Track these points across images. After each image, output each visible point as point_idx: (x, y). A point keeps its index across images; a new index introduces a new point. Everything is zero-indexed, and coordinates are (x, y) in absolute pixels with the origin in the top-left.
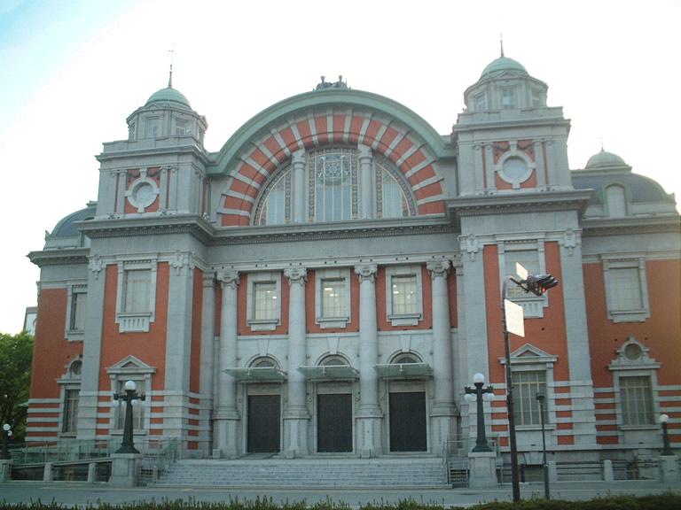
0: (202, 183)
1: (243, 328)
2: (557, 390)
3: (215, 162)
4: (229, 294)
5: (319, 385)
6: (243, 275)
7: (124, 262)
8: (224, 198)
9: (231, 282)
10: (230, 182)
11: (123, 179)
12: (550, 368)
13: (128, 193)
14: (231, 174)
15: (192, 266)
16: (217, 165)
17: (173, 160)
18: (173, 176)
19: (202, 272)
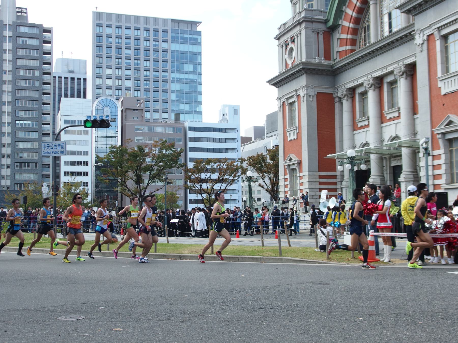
0: (321, 37)
1: (354, 127)
3: (327, 19)
4: (346, 104)
5: (392, 159)
6: (352, 90)
7: (287, 98)
8: (339, 40)
10: (340, 28)
11: (284, 48)
13: (287, 56)
14: (340, 23)
15: (313, 93)
16: (329, 21)
17: (298, 28)
18: (299, 38)
19: (332, 94)
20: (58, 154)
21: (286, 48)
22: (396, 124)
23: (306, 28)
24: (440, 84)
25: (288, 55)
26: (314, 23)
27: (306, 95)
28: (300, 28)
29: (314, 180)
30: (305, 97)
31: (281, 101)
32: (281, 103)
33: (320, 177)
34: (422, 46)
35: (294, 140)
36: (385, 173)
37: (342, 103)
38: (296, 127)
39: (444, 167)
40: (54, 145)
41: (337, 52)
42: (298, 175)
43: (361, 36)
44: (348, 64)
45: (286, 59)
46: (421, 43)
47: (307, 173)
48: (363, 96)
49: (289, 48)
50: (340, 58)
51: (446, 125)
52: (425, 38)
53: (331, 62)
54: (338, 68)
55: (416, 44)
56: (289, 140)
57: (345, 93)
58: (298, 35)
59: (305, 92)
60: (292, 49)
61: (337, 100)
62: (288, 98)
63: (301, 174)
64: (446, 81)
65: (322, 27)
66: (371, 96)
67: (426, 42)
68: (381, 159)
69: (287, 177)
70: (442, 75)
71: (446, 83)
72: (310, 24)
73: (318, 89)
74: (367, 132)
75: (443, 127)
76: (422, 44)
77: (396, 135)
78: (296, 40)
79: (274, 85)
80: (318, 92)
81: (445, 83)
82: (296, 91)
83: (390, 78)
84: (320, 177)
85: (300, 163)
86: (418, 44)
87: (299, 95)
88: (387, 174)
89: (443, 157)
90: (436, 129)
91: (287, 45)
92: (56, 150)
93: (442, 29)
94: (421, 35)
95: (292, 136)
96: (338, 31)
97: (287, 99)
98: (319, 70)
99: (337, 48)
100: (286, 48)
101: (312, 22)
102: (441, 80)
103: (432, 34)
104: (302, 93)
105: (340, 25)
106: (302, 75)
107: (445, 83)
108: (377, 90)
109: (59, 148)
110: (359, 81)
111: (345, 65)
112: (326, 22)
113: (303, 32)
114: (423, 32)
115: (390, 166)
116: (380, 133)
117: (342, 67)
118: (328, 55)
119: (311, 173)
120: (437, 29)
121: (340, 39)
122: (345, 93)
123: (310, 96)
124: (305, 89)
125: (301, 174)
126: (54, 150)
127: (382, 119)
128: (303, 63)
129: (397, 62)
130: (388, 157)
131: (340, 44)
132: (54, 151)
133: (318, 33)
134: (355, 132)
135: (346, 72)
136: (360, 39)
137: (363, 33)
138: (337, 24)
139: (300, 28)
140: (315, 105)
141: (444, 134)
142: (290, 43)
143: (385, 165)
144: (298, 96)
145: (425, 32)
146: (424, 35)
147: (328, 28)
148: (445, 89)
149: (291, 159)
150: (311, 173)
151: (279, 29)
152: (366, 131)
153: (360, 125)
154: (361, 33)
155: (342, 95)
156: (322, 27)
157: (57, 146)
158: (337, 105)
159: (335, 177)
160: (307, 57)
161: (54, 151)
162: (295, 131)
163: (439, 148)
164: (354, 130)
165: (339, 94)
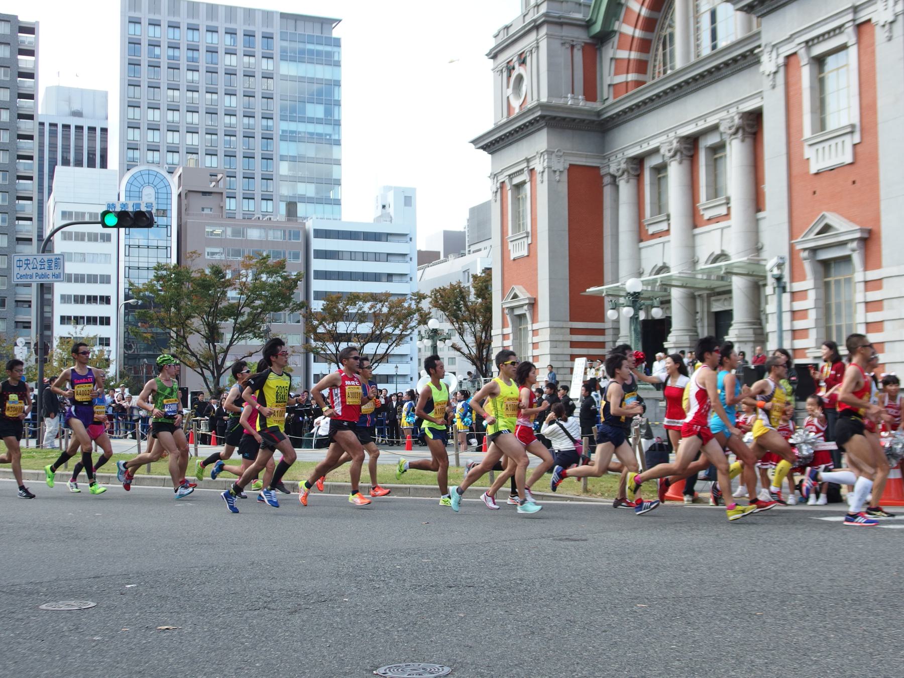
0: (578, 55)
1: (641, 235)
2: (869, 285)
3: (590, 20)
4: (626, 189)
5: (713, 298)
6: (639, 161)
7: (509, 176)
8: (613, 63)
9: (623, 173)
10: (616, 39)
11: (505, 74)
12: (853, 250)
13: (510, 91)
14: (616, 28)
15: (561, 165)
16: (595, 23)
17: (532, 37)
18: (534, 55)
20: (48, 280)
21: (509, 76)
22: (722, 229)
23: (549, 36)
24: (808, 153)
25: (514, 88)
26: (565, 28)
27: (546, 170)
28: (537, 35)
29: (561, 338)
30: (546, 175)
31: (497, 181)
32: (498, 185)
33: (573, 331)
34: (774, 78)
35: (523, 257)
36: (699, 325)
37: (617, 187)
38: (527, 233)
39: (812, 315)
40: (38, 261)
41: (609, 85)
42: (530, 327)
43: (656, 55)
44: (631, 109)
45: (508, 97)
46: (774, 70)
47: (547, 324)
48: (659, 174)
49: (514, 74)
50: (615, 98)
51: (818, 233)
52: (781, 60)
53: (597, 106)
54: (611, 118)
55: (763, 73)
56: (512, 258)
57: (623, 166)
58: (533, 51)
59: (545, 164)
60: (520, 78)
61: (607, 180)
62: (512, 174)
63: (536, 326)
64: (820, 146)
65: (581, 36)
66: (675, 173)
67: (782, 70)
68: (692, 298)
69: (508, 330)
70: (812, 134)
71: (820, 151)
72: (556, 30)
73: (571, 158)
74: (666, 244)
75: (812, 236)
76: (775, 73)
77: (722, 251)
78: (528, 60)
79: (484, 148)
80: (570, 165)
81: (817, 150)
82: (528, 160)
83: (712, 140)
84: (573, 331)
85: (533, 305)
86: (767, 73)
87: (534, 169)
88: (703, 327)
89: (812, 295)
90: (799, 240)
91: (510, 69)
92: (43, 271)
93: (813, 45)
94: (774, 54)
95: (518, 251)
96: (611, 44)
97: (511, 176)
98: (574, 120)
99: (609, 77)
100: (509, 76)
101: (561, 24)
102: (811, 145)
103: (795, 54)
104: (539, 165)
105: (614, 32)
106: (539, 130)
107: (817, 150)
108: (686, 163)
109: (50, 268)
110: (651, 143)
111: (624, 112)
112: (588, 25)
113: (543, 45)
114: (778, 49)
115: (709, 312)
116: (691, 246)
117: (618, 115)
118: (591, 92)
119: (556, 324)
120: (803, 45)
121: (616, 60)
122: (623, 166)
123: (555, 172)
124: (546, 157)
125: (536, 326)
126: (40, 272)
127: (694, 219)
128: (541, 106)
129: (726, 108)
130: (705, 293)
131: (616, 69)
132: (40, 274)
133: (573, 47)
134: (642, 244)
135: (628, 125)
136: (655, 60)
137: (661, 48)
138: (611, 29)
139: (537, 35)
140: (564, 188)
141: (814, 250)
142: (517, 66)
143: (699, 309)
144: (532, 171)
145: (781, 50)
146: (778, 55)
147: (593, 37)
148: (817, 161)
149: (515, 296)
150: (556, 324)
151: (496, 37)
152: (664, 243)
153: (652, 230)
154: (657, 50)
155: (618, 170)
156: (581, 36)
157: (46, 263)
158: (607, 191)
159: (601, 332)
160: (550, 95)
161: (40, 274)
162: (525, 239)
163: (803, 278)
164: (641, 241)
165: (613, 169)
